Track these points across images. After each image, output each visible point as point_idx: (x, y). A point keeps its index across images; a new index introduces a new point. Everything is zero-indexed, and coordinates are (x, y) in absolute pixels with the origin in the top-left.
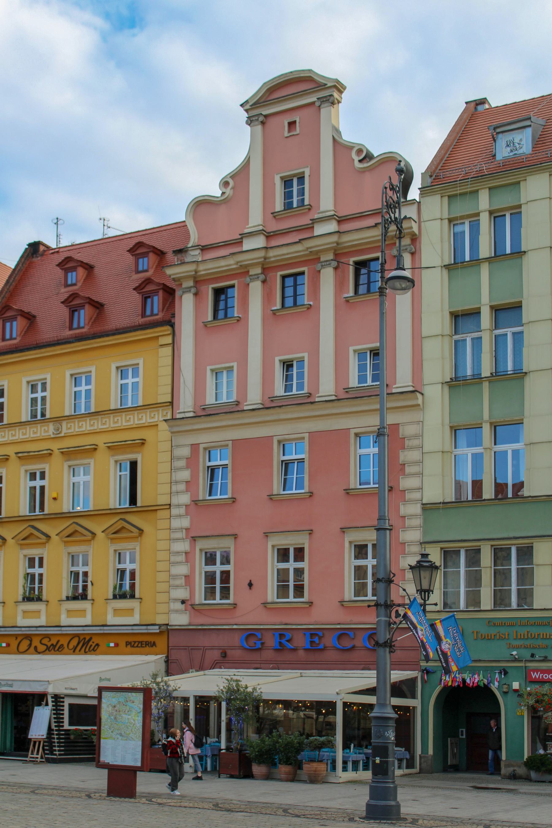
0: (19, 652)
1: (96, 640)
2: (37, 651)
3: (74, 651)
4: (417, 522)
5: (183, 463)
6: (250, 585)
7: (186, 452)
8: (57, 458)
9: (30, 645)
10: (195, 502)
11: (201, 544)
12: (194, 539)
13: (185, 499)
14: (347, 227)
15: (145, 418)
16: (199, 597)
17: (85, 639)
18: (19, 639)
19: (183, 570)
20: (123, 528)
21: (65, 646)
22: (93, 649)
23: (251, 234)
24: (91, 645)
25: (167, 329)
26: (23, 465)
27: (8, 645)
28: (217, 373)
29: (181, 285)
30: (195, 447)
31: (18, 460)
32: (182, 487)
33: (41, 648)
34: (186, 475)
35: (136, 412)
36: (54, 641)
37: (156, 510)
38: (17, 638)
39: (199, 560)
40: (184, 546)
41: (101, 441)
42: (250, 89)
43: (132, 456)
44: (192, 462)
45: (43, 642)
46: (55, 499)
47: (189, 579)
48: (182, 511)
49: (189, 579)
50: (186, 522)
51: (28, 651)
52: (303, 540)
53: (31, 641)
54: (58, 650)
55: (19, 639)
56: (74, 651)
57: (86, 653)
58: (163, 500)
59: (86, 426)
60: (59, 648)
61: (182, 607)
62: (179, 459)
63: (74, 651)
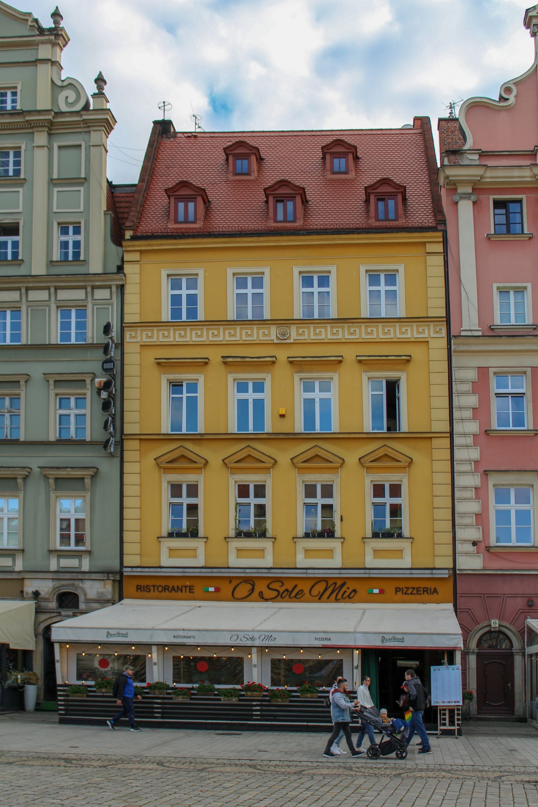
0: (234, 598)
1: (351, 585)
2: (262, 598)
3: (320, 599)
5: (468, 387)
9: (253, 590)
11: (493, 480)
12: (486, 473)
13: (473, 427)
15: (411, 332)
17: (336, 583)
18: (235, 583)
19: (474, 507)
20: (386, 455)
21: (307, 591)
22: (349, 596)
24: (345, 592)
26: (230, 373)
27: (217, 590)
28: (504, 292)
29: (456, 189)
31: (223, 365)
33: (269, 594)
34: (473, 400)
35: (397, 325)
36: (289, 586)
37: (431, 438)
38: (231, 581)
43: (392, 375)
45: (272, 586)
46: (282, 416)
48: (470, 440)
50: (475, 454)
51: (248, 598)
53: (253, 586)
54: (295, 596)
55: (235, 583)
56: (320, 598)
57: (337, 600)
59: (326, 333)
60: (297, 594)
63: (320, 599)
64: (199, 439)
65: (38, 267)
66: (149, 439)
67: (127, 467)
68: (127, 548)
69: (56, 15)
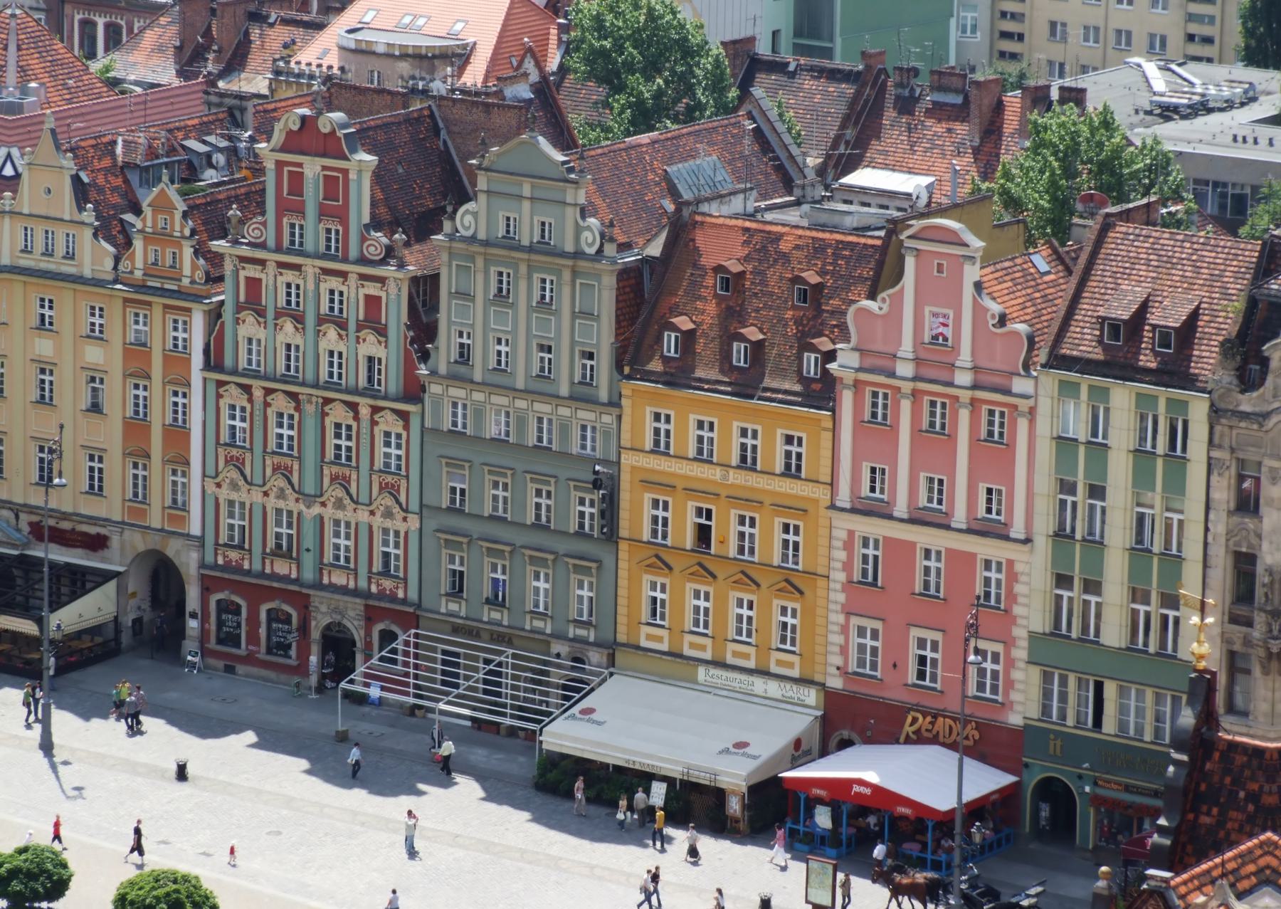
4: (1025, 644)
6: (895, 666)
7: (843, 535)
10: (850, 582)
11: (855, 621)
12: (848, 614)
19: (839, 639)
39: (853, 633)
40: (841, 618)
44: (848, 546)
49: (844, 650)
58: (820, 571)
61: (837, 672)
62: (838, 539)
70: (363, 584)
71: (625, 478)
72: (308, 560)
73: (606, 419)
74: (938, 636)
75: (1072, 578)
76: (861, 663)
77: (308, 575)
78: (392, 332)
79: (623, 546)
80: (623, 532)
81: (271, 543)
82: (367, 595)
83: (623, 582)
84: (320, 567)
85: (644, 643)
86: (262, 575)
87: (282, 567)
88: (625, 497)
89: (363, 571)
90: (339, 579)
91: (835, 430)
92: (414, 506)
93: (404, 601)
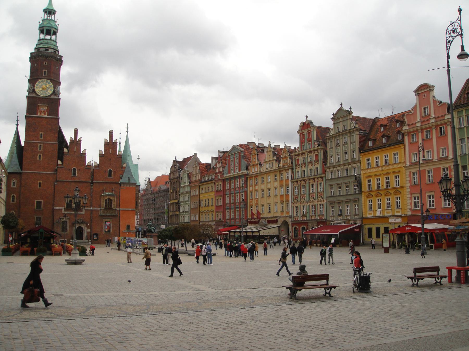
7: (408, 173)
8: (382, 175)
11: (413, 195)
12: (411, 194)
13: (409, 185)
14: (438, 119)
16: (413, 208)
19: (409, 201)
23: (418, 122)
25: (403, 144)
30: (410, 172)
32: (408, 182)
39: (413, 199)
40: (409, 196)
41: (391, 171)
42: (415, 88)
47: (411, 203)
48: (408, 187)
49: (411, 203)
52: (433, 194)
64: (371, 191)
65: (350, 161)
66: (365, 192)
67: (363, 198)
68: (364, 213)
69: (350, 108)
70: (317, 217)
71: (362, 176)
72: (308, 215)
73: (358, 164)
74: (433, 194)
75: (466, 166)
76: (415, 207)
77: (308, 218)
78: (320, 161)
79: (363, 193)
80: (363, 190)
81: (302, 213)
82: (318, 220)
83: (363, 202)
84: (310, 216)
85: (369, 216)
86: (301, 221)
87: (304, 219)
88: (362, 181)
89: (317, 215)
90: (313, 218)
91: (404, 148)
92: (325, 198)
93: (324, 219)
